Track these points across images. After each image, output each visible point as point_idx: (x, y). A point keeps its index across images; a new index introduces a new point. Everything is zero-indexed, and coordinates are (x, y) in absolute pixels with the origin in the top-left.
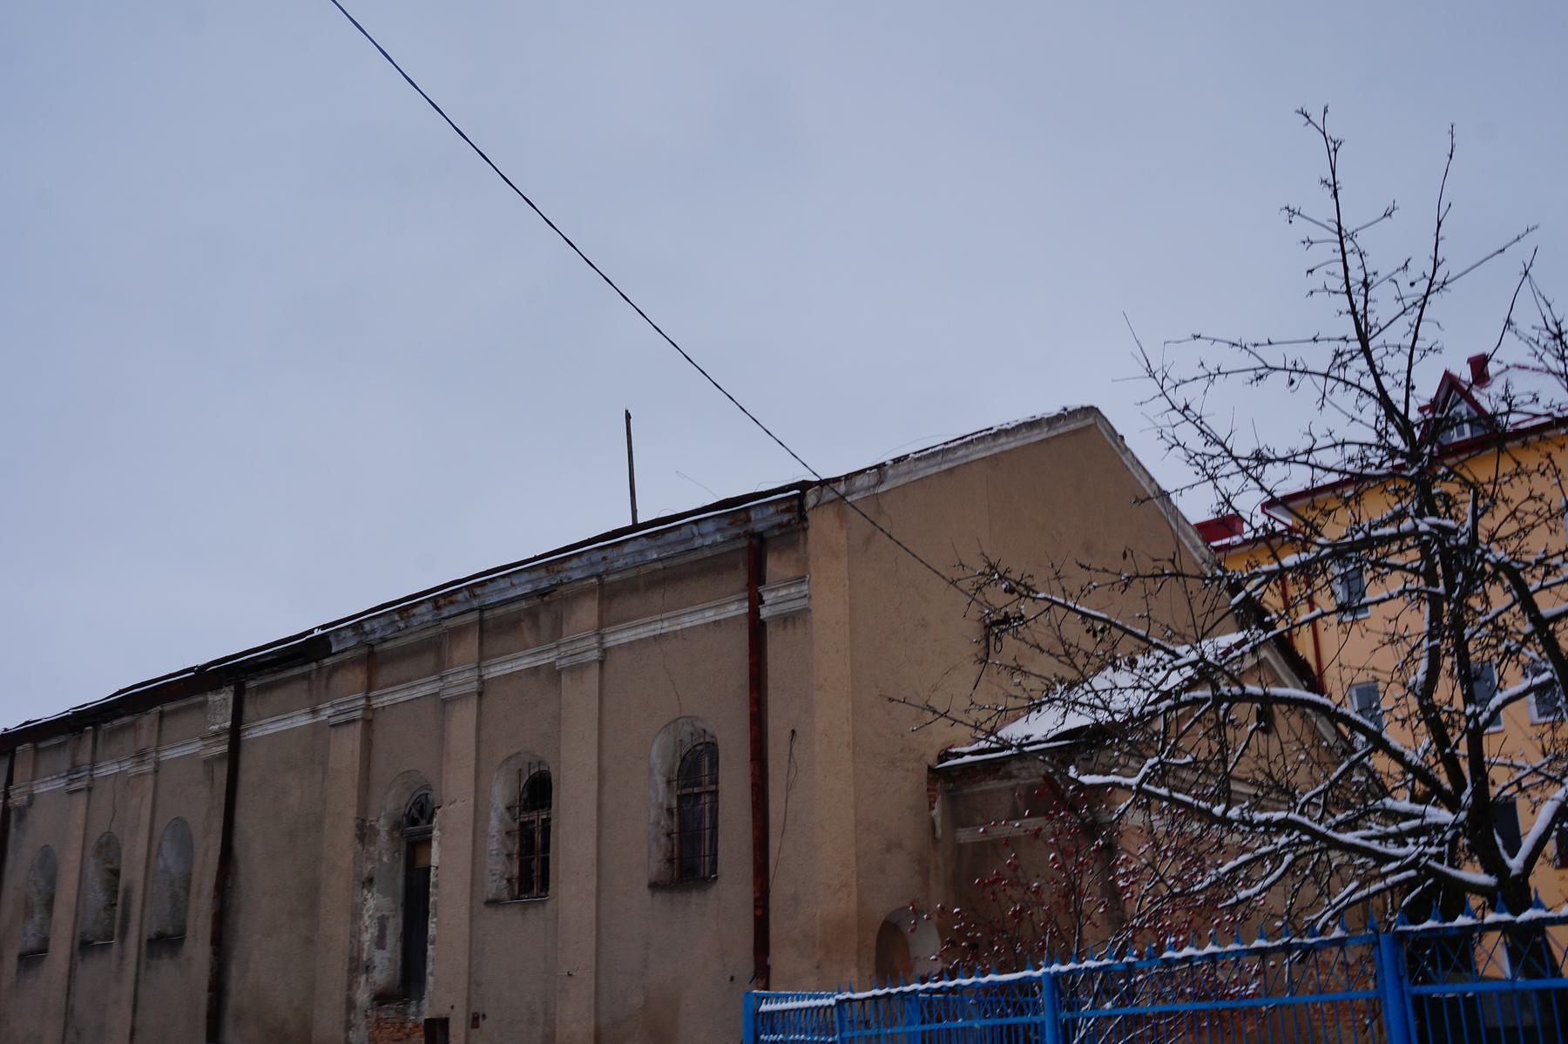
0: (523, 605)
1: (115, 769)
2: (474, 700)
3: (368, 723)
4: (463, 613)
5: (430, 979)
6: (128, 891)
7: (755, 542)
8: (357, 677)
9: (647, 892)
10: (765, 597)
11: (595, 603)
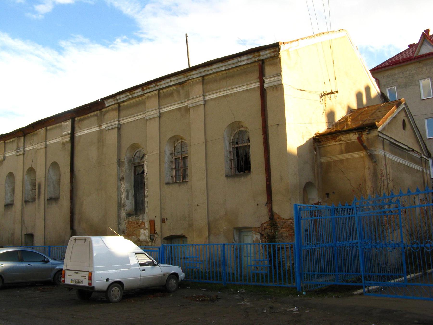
1: (31, 148)
2: (157, 119)
3: (119, 129)
5: (146, 209)
6: (40, 185)
7: (261, 63)
8: (115, 113)
9: (225, 178)
10: (266, 81)
11: (201, 86)
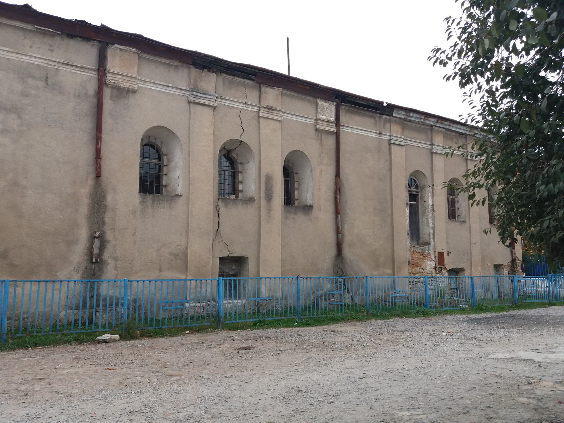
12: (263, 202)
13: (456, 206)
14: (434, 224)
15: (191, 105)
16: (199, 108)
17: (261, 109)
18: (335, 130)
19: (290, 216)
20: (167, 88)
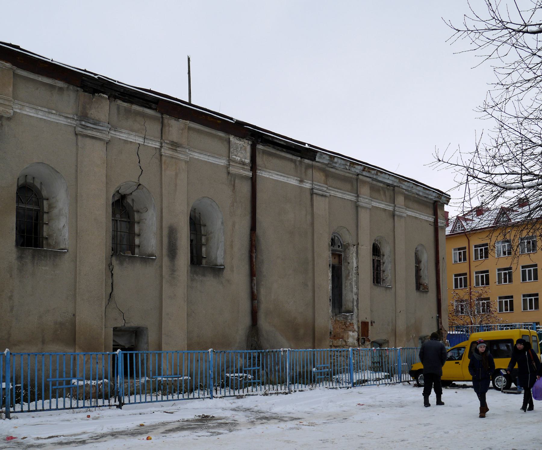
0: (382, 185)
4: (367, 177)
12: (166, 260)
13: (382, 269)
14: (358, 288)
15: (79, 137)
16: (88, 141)
17: (163, 145)
18: (250, 174)
19: (197, 278)
20: (50, 116)
